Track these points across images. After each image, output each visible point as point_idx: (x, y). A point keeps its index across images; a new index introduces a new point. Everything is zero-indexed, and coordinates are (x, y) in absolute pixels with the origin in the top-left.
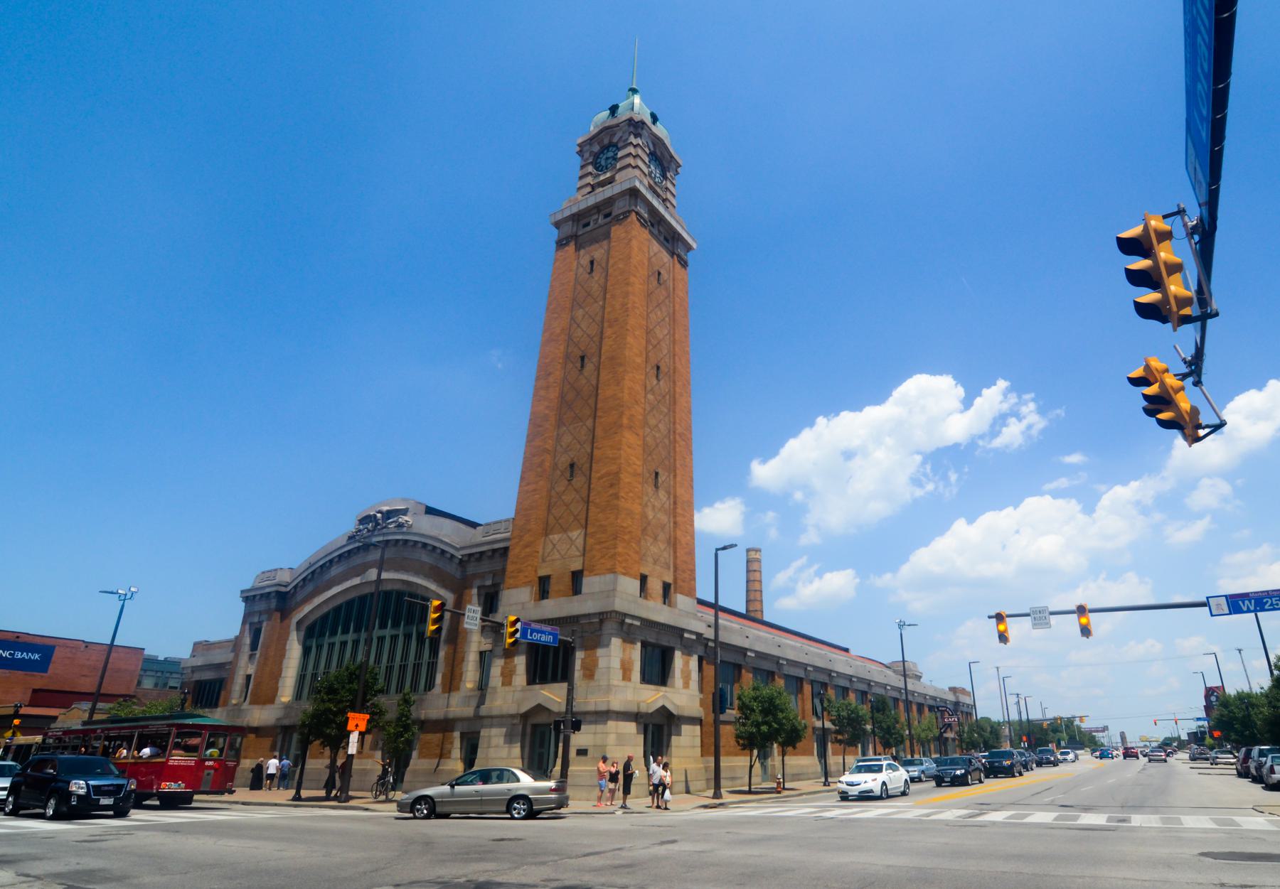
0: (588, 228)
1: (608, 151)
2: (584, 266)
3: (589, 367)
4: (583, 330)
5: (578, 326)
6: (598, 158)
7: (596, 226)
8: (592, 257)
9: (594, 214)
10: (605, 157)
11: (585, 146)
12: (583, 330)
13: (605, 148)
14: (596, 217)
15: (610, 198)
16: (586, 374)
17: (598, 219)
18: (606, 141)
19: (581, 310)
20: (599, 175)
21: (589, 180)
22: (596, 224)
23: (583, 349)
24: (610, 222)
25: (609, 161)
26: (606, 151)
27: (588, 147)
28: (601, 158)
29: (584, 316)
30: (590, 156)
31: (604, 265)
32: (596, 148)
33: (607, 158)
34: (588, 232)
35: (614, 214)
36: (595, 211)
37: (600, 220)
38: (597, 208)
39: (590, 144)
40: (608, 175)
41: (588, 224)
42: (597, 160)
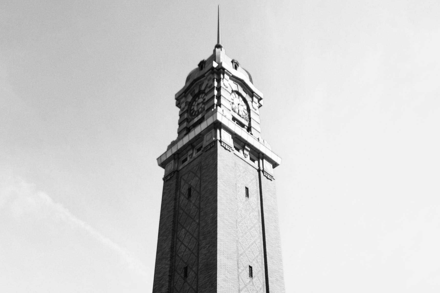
0: (186, 163)
1: (199, 98)
2: (185, 194)
3: (191, 274)
4: (185, 246)
5: (182, 243)
6: (192, 105)
7: (192, 159)
8: (190, 185)
9: (189, 150)
10: (196, 104)
11: (182, 98)
12: (185, 246)
13: (196, 97)
14: (191, 152)
15: (200, 134)
16: (189, 282)
17: (193, 153)
18: (197, 91)
19: (184, 230)
20: (193, 119)
21: (185, 124)
22: (191, 158)
23: (186, 261)
24: (202, 154)
25: (200, 105)
26: (197, 99)
27: (183, 99)
28: (194, 105)
29: (185, 234)
30: (186, 105)
31: (198, 190)
32: (190, 98)
33: (198, 104)
34: (186, 166)
35: (204, 147)
36: (190, 147)
37: (194, 155)
38: (191, 145)
39: (185, 96)
40: (200, 116)
41: (186, 160)
42: (191, 107)
